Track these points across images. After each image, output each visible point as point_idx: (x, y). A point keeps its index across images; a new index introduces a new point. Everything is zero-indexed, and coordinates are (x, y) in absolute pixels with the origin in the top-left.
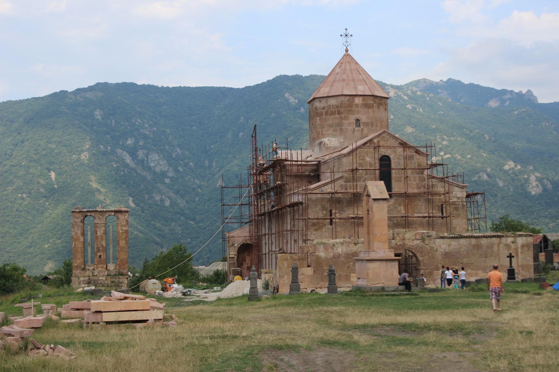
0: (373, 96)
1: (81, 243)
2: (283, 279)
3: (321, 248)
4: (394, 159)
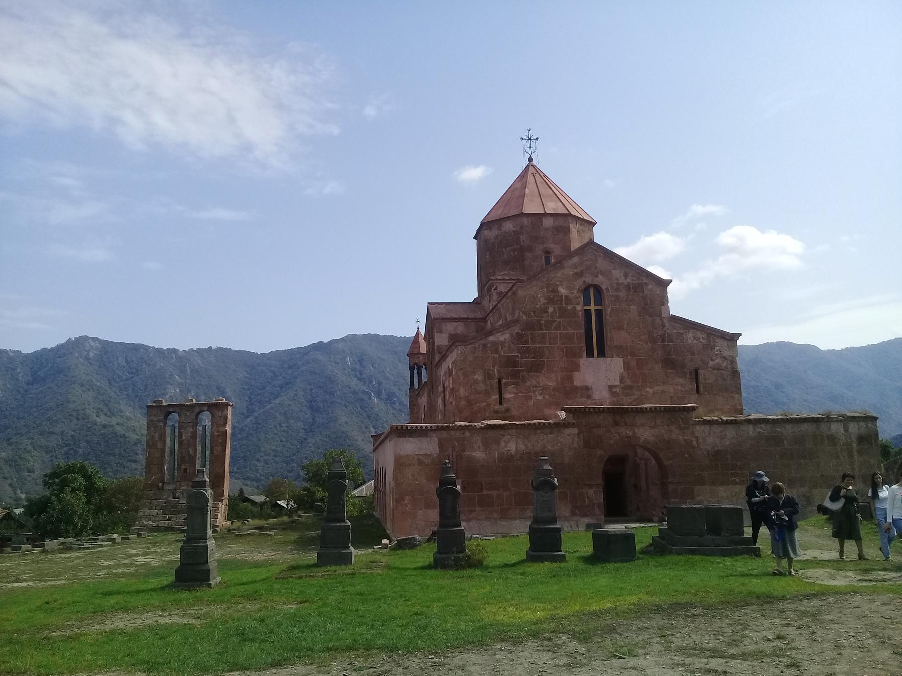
0: (570, 215)
1: (159, 450)
2: (403, 503)
3: (477, 440)
4: (607, 289)
